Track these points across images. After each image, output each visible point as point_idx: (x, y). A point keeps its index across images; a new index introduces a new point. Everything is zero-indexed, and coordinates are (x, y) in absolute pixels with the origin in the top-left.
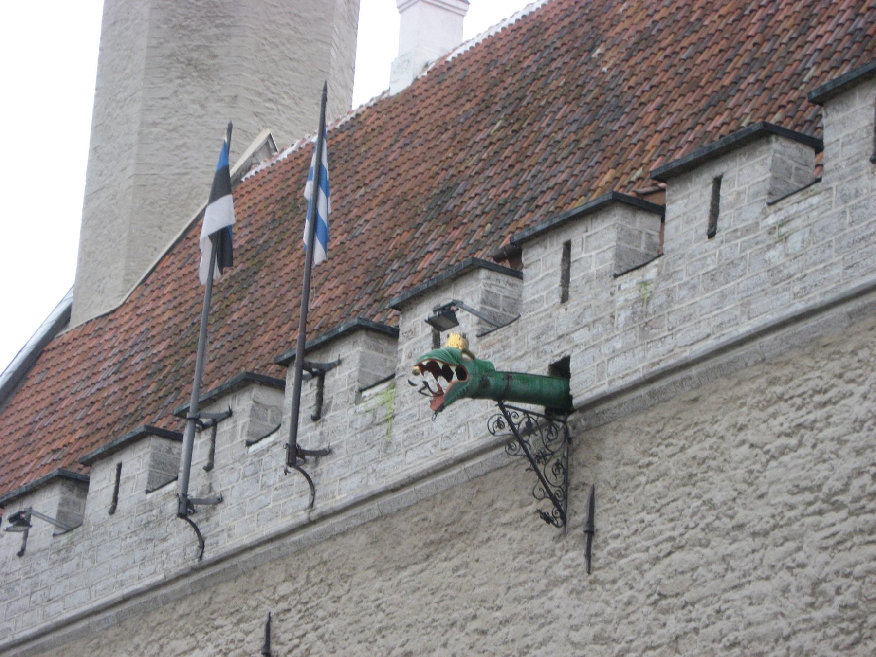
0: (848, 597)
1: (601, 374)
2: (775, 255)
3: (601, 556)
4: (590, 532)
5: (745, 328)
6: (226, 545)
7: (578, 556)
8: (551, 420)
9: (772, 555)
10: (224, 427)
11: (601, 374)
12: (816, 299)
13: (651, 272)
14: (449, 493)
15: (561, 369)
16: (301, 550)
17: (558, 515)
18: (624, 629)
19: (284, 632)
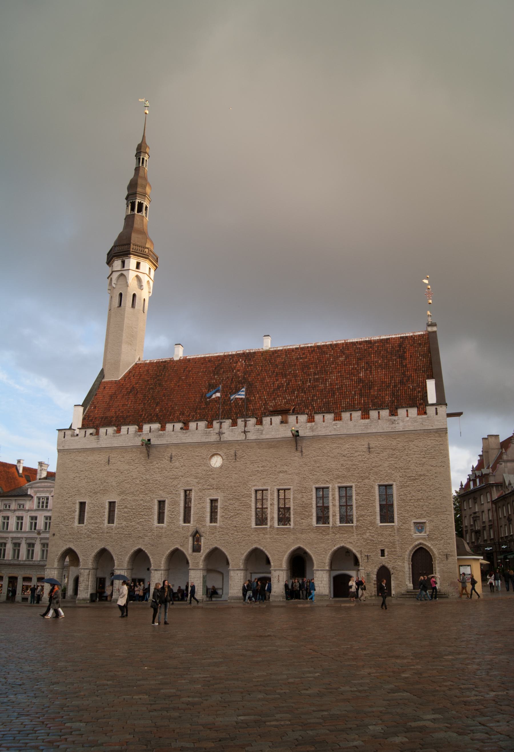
0: (347, 466)
1: (305, 433)
2: (335, 427)
3: (304, 455)
4: (302, 452)
5: (330, 434)
6: (225, 439)
7: (300, 454)
9: (334, 460)
10: (223, 424)
11: (305, 433)
12: (342, 433)
13: (313, 424)
14: (273, 442)
15: (297, 431)
16: (241, 443)
17: (296, 449)
18: (309, 464)
19: (239, 453)
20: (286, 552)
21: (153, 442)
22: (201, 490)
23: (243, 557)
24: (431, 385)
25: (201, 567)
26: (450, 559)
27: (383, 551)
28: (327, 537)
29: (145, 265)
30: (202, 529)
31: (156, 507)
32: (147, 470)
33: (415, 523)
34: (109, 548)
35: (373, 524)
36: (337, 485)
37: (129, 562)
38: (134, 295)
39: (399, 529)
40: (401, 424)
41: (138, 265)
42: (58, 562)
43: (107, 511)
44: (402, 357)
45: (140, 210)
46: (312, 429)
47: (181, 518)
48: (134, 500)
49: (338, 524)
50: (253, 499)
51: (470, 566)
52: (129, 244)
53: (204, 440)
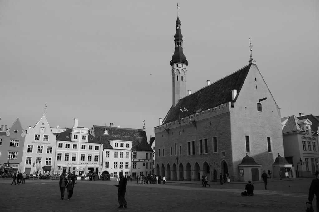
8: (194, 122)
15: (195, 120)
20: (194, 164)
21: (169, 129)
22: (178, 143)
23: (186, 166)
24: (235, 92)
25: (179, 169)
26: (231, 166)
27: (215, 163)
28: (202, 158)
29: (180, 65)
30: (179, 157)
31: (171, 150)
32: (169, 138)
33: (222, 152)
34: (164, 164)
35: (212, 153)
36: (204, 139)
37: (167, 168)
38: (178, 76)
39: (218, 154)
40: (218, 112)
41: (177, 65)
42: (157, 168)
43: (163, 152)
44: (237, 80)
45: (180, 44)
46: (198, 119)
47: (175, 153)
48: (167, 148)
49: (205, 153)
50: (187, 145)
51: (243, 169)
52: (179, 58)
53: (178, 126)
